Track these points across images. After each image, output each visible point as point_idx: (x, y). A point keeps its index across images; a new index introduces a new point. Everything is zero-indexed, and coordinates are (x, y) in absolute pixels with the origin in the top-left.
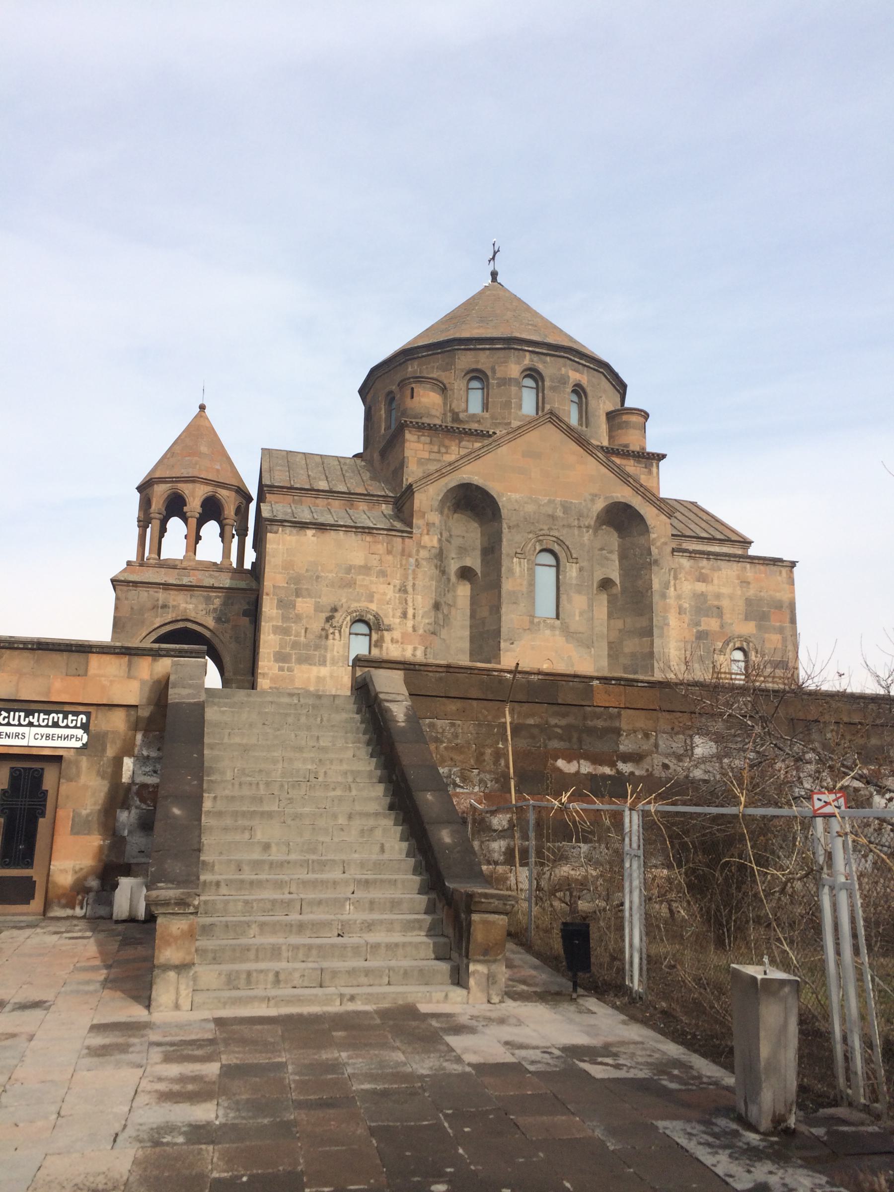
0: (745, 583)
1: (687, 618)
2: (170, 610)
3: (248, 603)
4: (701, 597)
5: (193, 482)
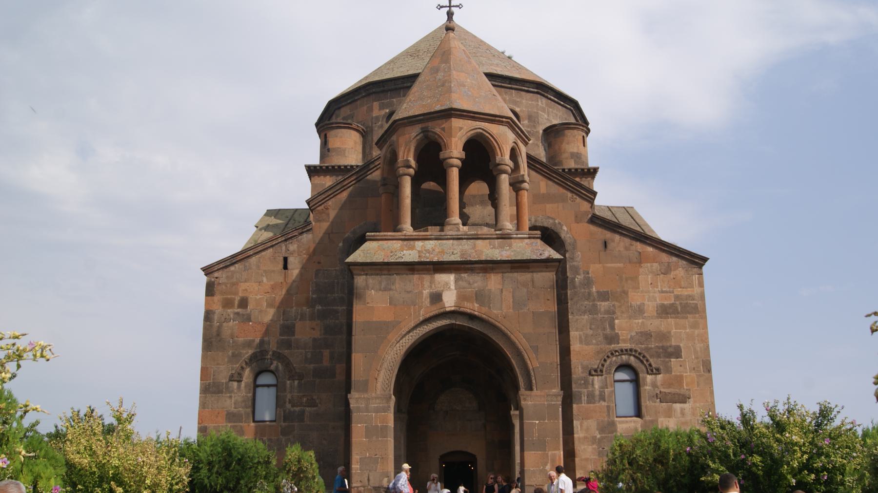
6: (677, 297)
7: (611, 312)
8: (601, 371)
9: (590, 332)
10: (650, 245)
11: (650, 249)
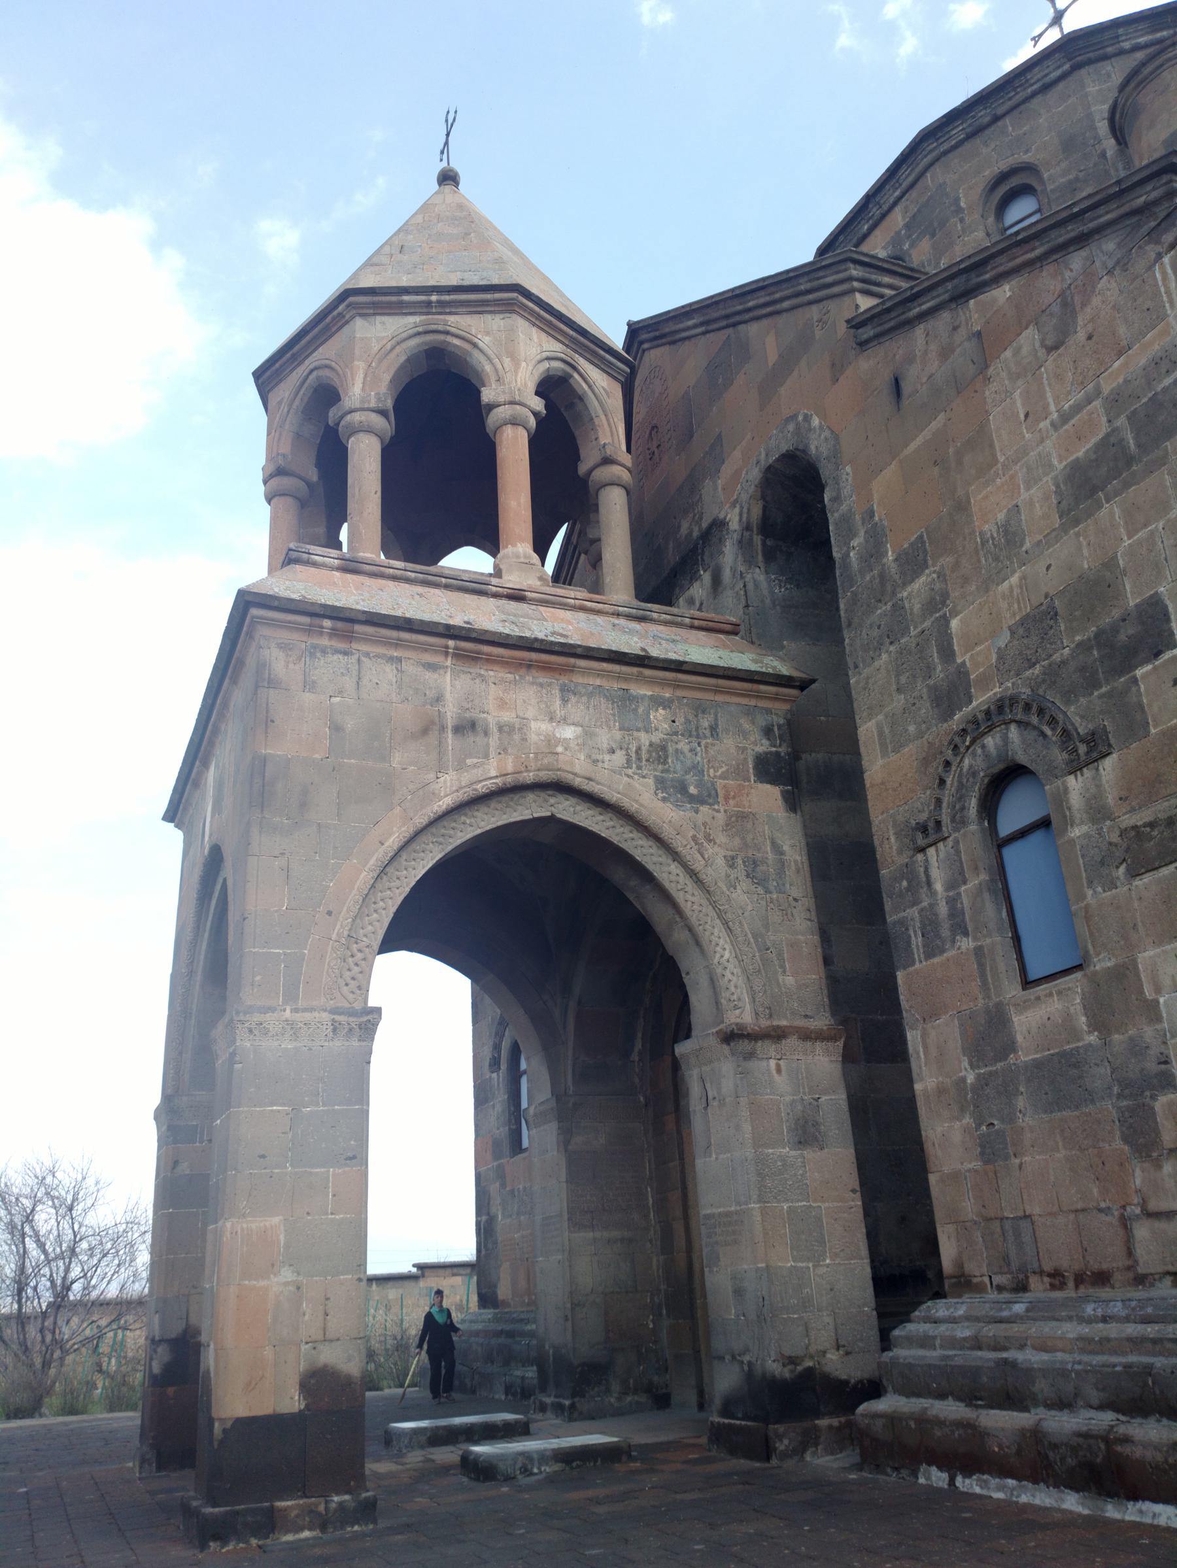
2: (494, 741)
3: (768, 732)
5: (508, 308)
6: (1115, 402)
7: (937, 603)
8: (938, 823)
9: (900, 701)
10: (997, 280)
11: (1004, 293)
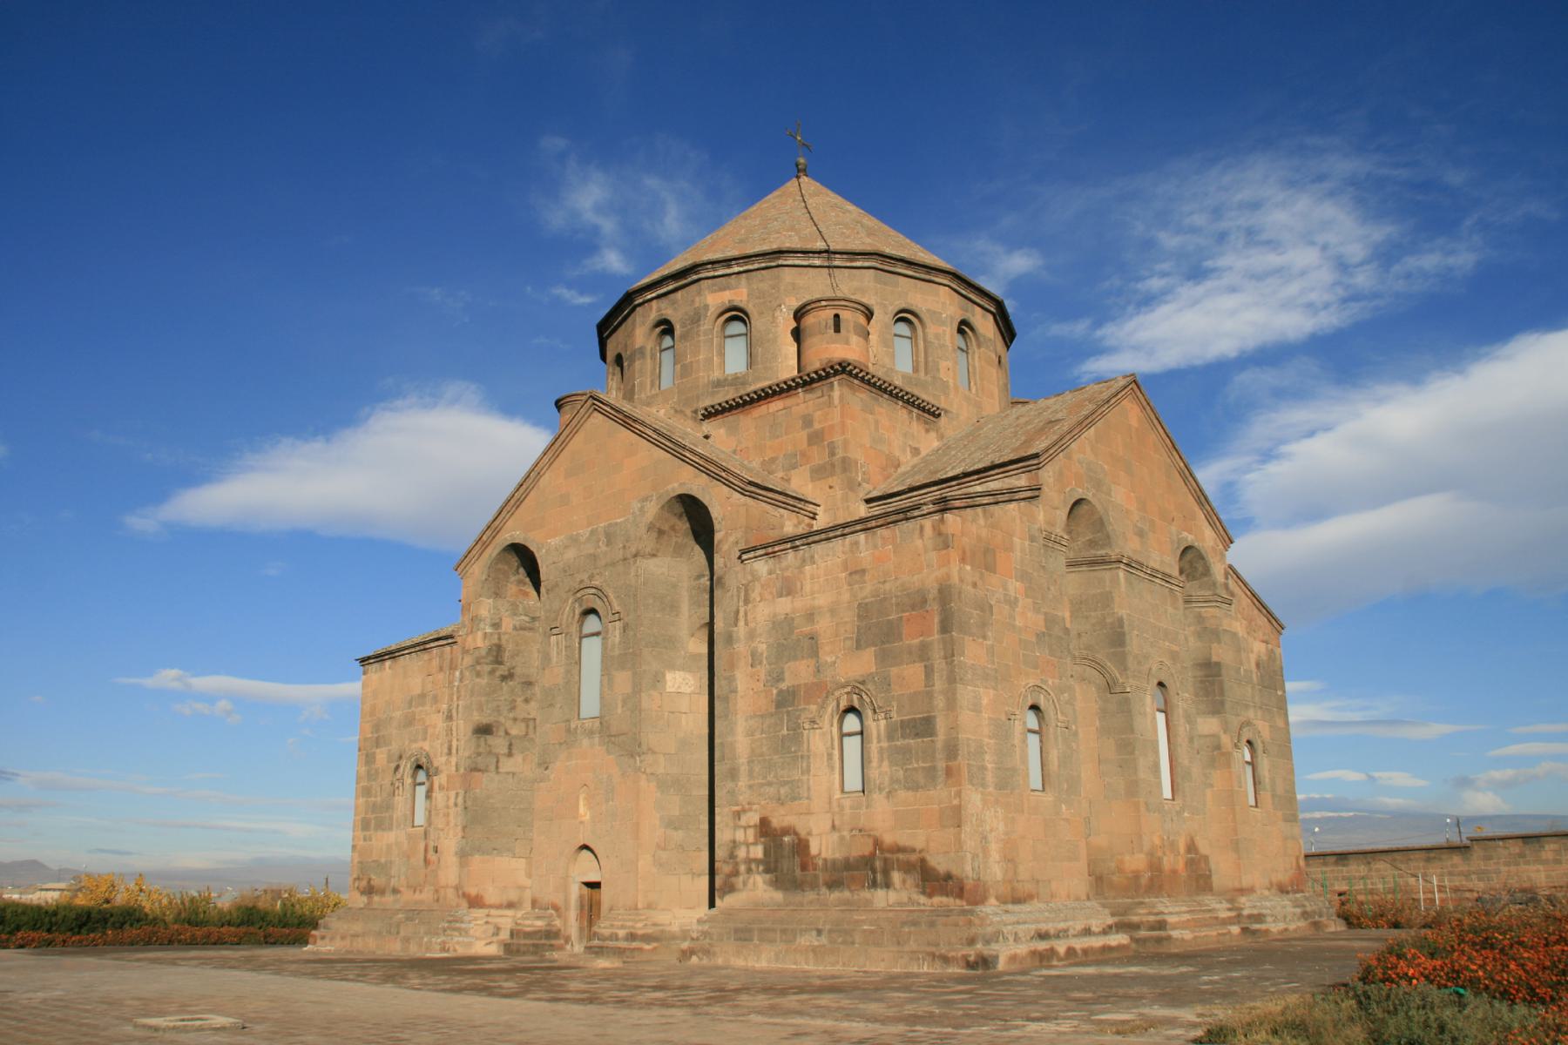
0: (857, 573)
1: (762, 671)
4: (782, 626)
